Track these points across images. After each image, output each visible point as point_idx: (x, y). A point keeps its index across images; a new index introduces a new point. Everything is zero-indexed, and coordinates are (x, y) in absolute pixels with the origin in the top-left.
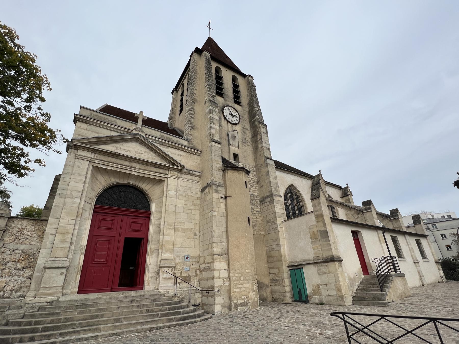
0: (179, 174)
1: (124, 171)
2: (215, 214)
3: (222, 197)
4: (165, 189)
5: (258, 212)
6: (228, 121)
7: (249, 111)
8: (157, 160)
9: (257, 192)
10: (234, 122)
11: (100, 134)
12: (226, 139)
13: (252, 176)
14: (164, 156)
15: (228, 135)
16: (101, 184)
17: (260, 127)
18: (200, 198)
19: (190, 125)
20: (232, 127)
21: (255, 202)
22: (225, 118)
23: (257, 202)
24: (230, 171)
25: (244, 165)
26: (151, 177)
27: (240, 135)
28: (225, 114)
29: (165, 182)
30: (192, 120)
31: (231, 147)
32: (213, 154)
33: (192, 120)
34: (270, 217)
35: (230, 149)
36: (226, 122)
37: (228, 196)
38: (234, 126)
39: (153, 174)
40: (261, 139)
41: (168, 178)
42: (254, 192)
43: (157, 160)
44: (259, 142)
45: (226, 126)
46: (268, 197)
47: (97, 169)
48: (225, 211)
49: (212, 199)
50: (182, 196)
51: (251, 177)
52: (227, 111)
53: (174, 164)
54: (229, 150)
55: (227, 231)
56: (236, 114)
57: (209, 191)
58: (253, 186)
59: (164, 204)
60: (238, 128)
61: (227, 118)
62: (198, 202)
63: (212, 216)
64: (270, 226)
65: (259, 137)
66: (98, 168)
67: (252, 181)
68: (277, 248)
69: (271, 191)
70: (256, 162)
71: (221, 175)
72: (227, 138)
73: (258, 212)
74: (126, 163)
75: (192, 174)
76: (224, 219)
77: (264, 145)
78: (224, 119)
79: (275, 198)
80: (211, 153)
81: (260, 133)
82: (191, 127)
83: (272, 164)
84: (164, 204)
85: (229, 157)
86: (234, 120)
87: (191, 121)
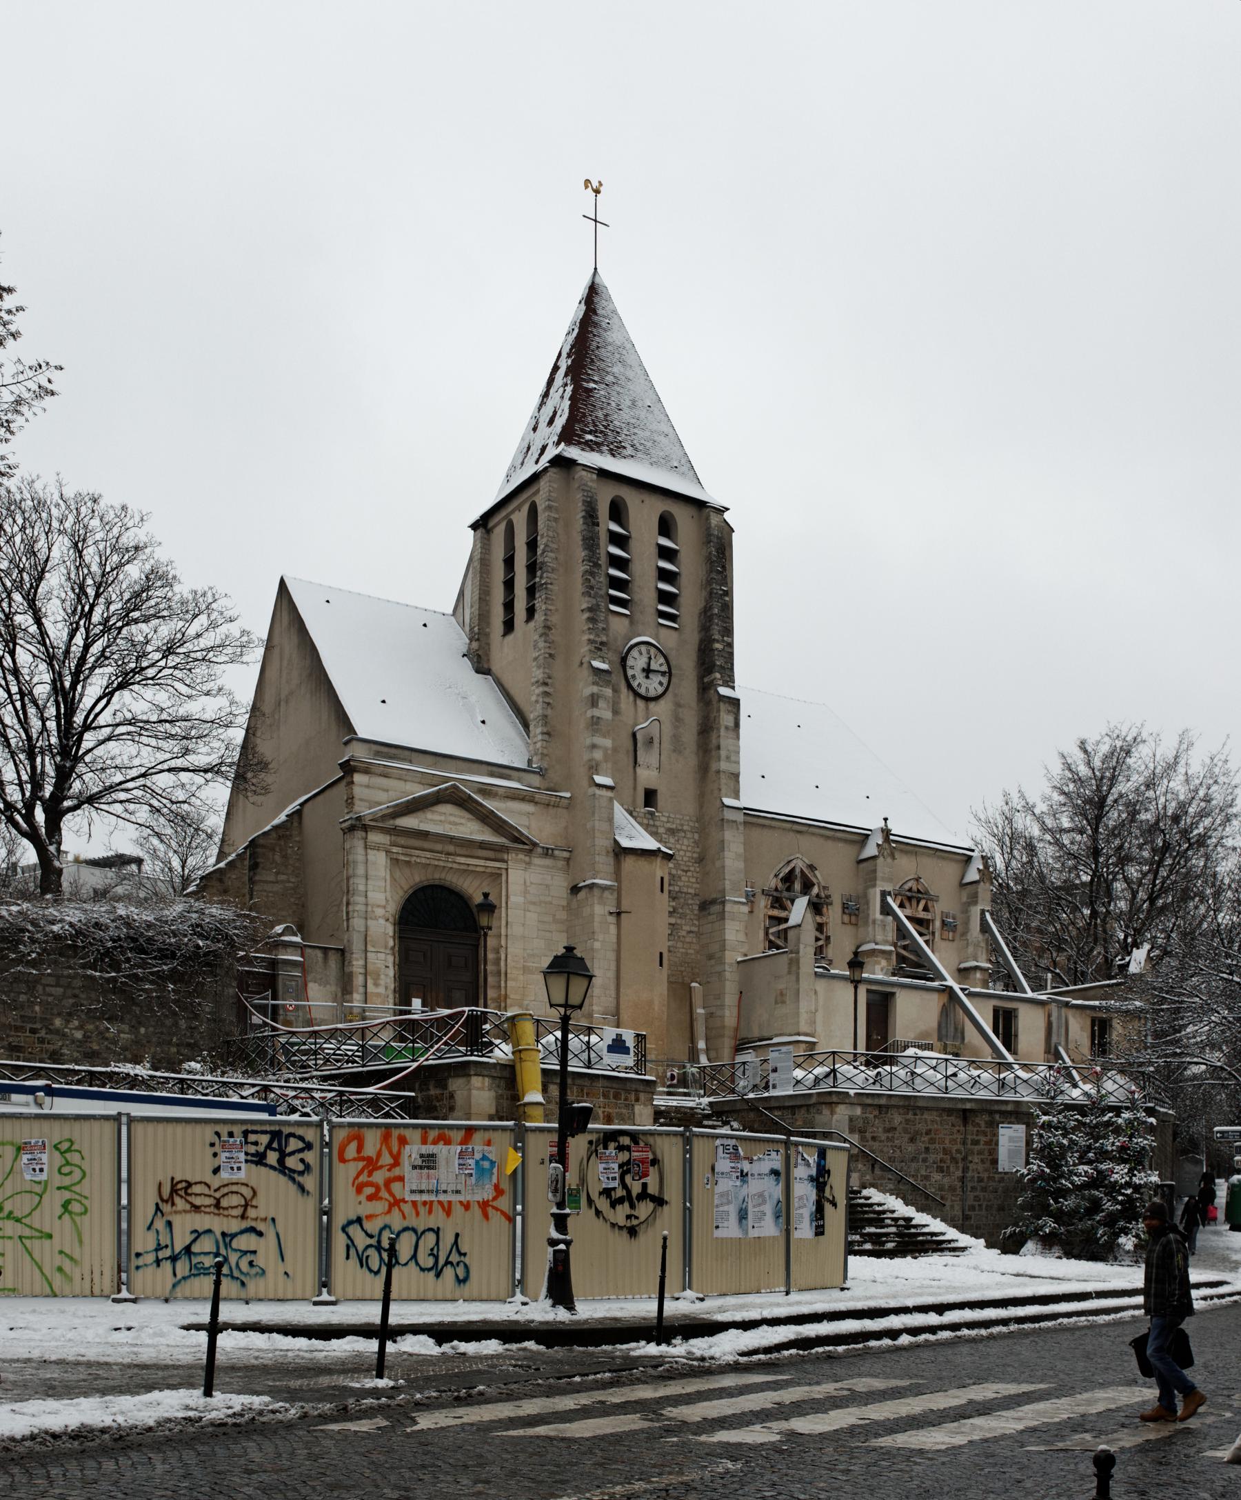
0: (527, 859)
1: (436, 863)
2: (597, 945)
3: (611, 913)
4: (504, 893)
5: (692, 932)
6: (637, 694)
7: (701, 641)
8: (487, 836)
9: (695, 886)
10: (652, 693)
11: (390, 793)
12: (628, 751)
13: (688, 846)
14: (497, 825)
15: (634, 735)
16: (402, 888)
17: (719, 711)
18: (568, 908)
19: (545, 730)
20: (647, 708)
21: (688, 911)
22: (630, 687)
23: (692, 910)
24: (630, 856)
25: (669, 817)
26: (478, 869)
27: (667, 729)
28: (630, 672)
29: (504, 878)
30: (549, 712)
31: (639, 770)
32: (597, 817)
33: (549, 712)
34: (715, 948)
35: (638, 780)
36: (631, 698)
37: (623, 910)
38: (652, 705)
39: (482, 862)
40: (719, 748)
41: (507, 869)
42: (688, 887)
43: (487, 836)
44: (714, 753)
45: (632, 709)
46: (713, 902)
47: (395, 861)
48: (615, 940)
49: (592, 915)
50: (534, 903)
51: (684, 848)
52: (637, 662)
53: (516, 840)
54: (635, 780)
55: (618, 977)
56: (661, 665)
57: (587, 899)
58: (686, 871)
59: (503, 923)
60: (662, 709)
61: (635, 684)
62: (562, 915)
63: (592, 949)
64: (712, 966)
65: (714, 735)
66: (397, 860)
67: (685, 859)
68: (719, 1013)
69: (723, 891)
70: (701, 806)
71: (612, 863)
72: (631, 748)
73: (691, 935)
74: (439, 847)
75: (553, 856)
76: (612, 956)
77: (724, 765)
78: (626, 690)
79: (728, 907)
80: (593, 813)
81: (718, 729)
82: (548, 734)
83: (735, 822)
84: (503, 923)
85: (634, 801)
86: (653, 686)
87: (546, 716)
